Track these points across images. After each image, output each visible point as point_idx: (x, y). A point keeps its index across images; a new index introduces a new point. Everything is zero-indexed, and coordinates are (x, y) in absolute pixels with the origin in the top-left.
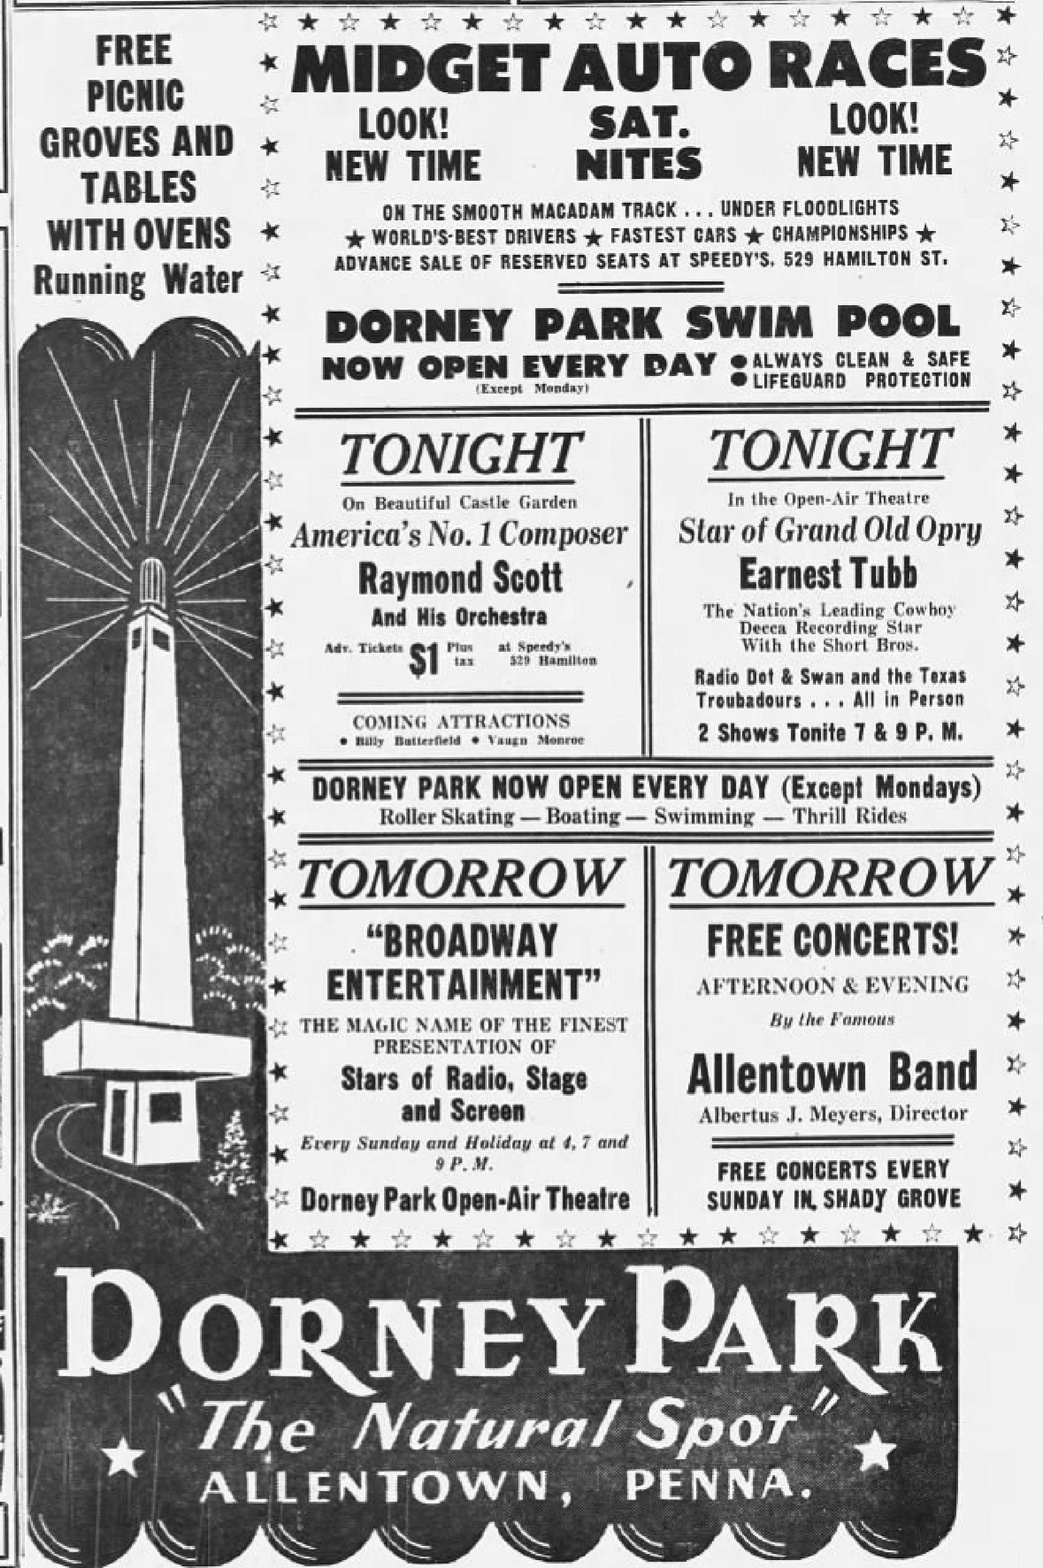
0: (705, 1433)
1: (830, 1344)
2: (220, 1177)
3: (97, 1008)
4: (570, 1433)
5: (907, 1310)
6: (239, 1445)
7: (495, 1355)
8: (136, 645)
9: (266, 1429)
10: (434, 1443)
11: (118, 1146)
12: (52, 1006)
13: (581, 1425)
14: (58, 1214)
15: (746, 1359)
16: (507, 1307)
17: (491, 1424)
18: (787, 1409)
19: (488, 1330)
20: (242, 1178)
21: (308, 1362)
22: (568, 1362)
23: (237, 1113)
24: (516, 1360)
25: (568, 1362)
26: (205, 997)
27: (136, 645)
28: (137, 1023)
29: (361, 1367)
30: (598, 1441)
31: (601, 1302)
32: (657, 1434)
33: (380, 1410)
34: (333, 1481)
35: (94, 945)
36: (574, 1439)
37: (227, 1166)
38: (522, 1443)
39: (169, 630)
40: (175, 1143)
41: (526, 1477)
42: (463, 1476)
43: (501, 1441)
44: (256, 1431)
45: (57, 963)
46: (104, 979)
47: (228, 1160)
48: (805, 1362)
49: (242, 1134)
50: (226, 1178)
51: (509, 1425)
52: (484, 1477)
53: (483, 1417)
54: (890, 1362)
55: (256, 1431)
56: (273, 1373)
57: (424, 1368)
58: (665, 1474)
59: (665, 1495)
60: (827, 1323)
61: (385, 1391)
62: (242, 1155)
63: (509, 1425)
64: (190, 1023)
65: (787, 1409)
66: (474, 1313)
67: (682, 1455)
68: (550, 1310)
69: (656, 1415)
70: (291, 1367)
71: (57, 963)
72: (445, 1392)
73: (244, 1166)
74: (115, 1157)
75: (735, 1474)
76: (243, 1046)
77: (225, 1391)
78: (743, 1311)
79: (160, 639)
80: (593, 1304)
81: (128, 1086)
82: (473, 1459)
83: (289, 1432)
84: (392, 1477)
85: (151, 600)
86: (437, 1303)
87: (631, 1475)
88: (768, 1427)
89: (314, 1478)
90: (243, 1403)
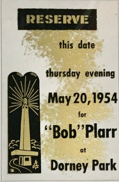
3: (18, 148)
11: (21, 163)
28: (23, 150)
39: (28, 107)
64: (30, 150)
79: (26, 108)
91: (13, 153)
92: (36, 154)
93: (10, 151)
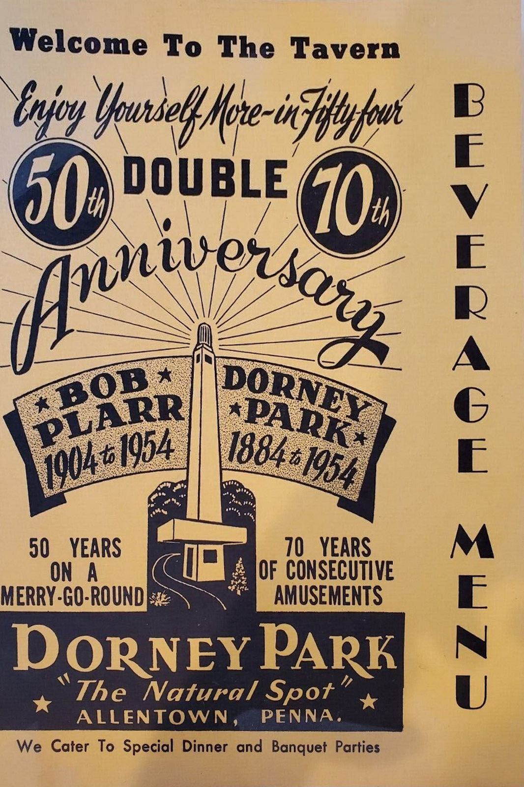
0: (295, 694)
1: (348, 657)
2: (234, 587)
3: (180, 513)
4: (236, 695)
5: (381, 643)
6: (93, 698)
7: (204, 661)
8: (198, 361)
9: (105, 692)
10: (178, 698)
11: (190, 573)
12: (162, 513)
13: (241, 691)
14: (164, 601)
15: (313, 664)
16: (208, 641)
17: (202, 690)
18: (330, 684)
19: (201, 651)
20: (243, 587)
21: (123, 664)
22: (235, 665)
23: (241, 559)
24: (213, 663)
25: (235, 665)
26: (227, 510)
27: (198, 361)
28: (198, 521)
29: (146, 666)
30: (249, 698)
31: (249, 639)
32: (275, 695)
33: (154, 684)
34: (135, 715)
35: (180, 487)
36: (238, 697)
37: (236, 583)
38: (216, 698)
40: (213, 572)
41: (218, 713)
42: (190, 713)
43: (207, 697)
44: (101, 693)
45: (164, 494)
46: (184, 501)
47: (237, 580)
48: (338, 665)
49: (243, 568)
50: (236, 588)
51: (210, 690)
52: (200, 713)
53: (199, 688)
54: (374, 664)
55: (101, 693)
56: (108, 668)
57: (173, 667)
58: (278, 712)
59: (278, 721)
60: (347, 648)
61: (156, 676)
62: (243, 578)
63: (210, 690)
64: (221, 521)
65: (330, 684)
66: (194, 643)
67: (285, 703)
68: (227, 642)
69: (273, 687)
70: (115, 665)
71: (164, 494)
72: (184, 677)
73: (243, 582)
74: (189, 578)
75: (308, 711)
76: (244, 531)
77: (86, 676)
78: (310, 643)
80: (245, 640)
81: (194, 547)
82: (195, 705)
83: (115, 693)
84: (160, 713)
85: (204, 342)
86: (178, 639)
87: (264, 711)
88: (322, 692)
89: (126, 712)
90: (95, 681)
91: (164, 533)
92: (239, 535)
93: (154, 523)
